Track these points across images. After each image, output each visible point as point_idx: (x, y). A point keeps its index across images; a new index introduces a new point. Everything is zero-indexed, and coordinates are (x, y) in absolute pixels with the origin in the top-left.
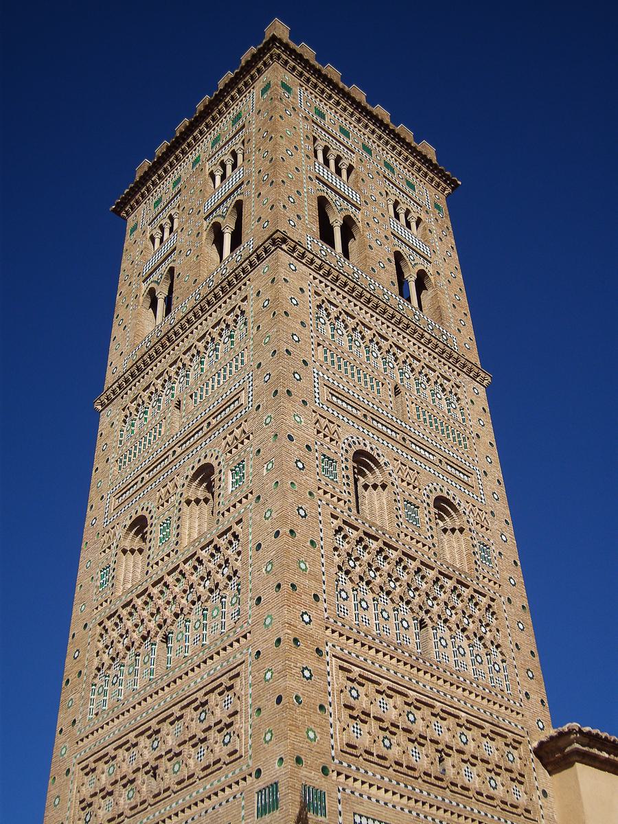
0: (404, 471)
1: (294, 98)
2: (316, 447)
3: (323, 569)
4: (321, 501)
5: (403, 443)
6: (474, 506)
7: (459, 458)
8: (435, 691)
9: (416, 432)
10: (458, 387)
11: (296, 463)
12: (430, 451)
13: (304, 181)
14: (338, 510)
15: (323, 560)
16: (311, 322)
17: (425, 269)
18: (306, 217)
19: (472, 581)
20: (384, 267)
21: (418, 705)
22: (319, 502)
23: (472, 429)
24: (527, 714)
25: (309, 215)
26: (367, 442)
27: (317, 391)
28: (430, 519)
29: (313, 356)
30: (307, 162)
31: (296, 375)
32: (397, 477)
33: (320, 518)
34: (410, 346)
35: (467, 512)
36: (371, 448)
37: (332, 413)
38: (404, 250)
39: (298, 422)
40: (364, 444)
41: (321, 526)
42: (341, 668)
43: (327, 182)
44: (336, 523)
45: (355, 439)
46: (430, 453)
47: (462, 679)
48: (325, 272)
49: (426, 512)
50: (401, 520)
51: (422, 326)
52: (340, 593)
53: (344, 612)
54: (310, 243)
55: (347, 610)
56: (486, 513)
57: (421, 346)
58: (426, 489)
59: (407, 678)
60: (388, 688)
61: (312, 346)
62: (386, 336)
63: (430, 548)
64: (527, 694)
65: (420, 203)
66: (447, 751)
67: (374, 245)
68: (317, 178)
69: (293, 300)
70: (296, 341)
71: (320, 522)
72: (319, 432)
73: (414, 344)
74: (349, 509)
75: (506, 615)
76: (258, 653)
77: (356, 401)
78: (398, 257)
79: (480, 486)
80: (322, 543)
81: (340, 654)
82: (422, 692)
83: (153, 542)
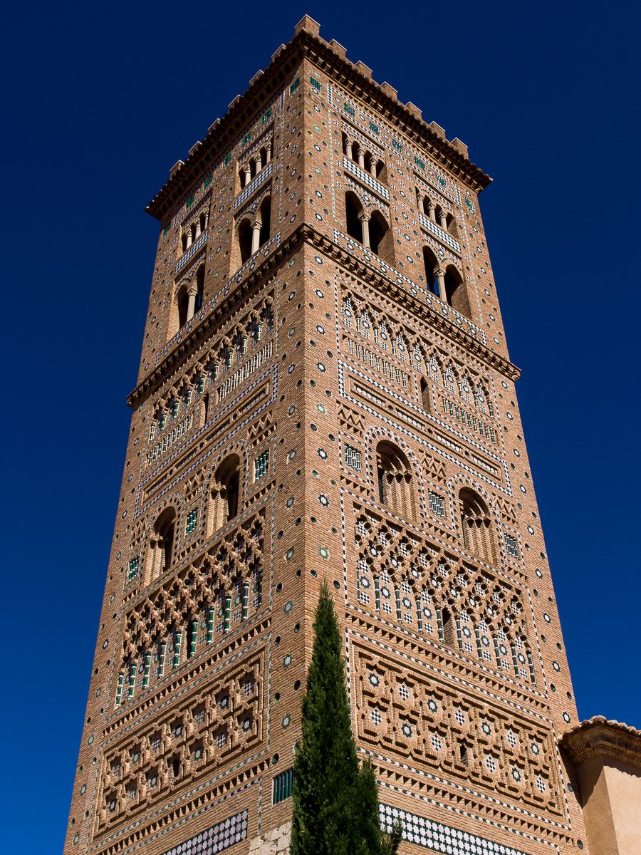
0: (428, 462)
1: (323, 94)
2: (340, 437)
3: (344, 556)
4: (343, 489)
5: (428, 434)
6: (501, 498)
7: (485, 450)
8: (457, 679)
9: (442, 424)
10: (487, 381)
11: (319, 451)
12: (456, 443)
13: (332, 176)
14: (361, 499)
15: (344, 548)
16: (336, 314)
17: (454, 264)
18: (334, 212)
19: (497, 572)
20: (412, 262)
21: (440, 693)
22: (342, 491)
23: (499, 422)
24: (552, 706)
25: (336, 209)
26: (392, 433)
27: (341, 382)
28: (455, 510)
29: (338, 347)
30: (335, 158)
31: (320, 366)
32: (421, 468)
33: (342, 506)
34: (437, 340)
35: (493, 504)
36: (396, 439)
37: (355, 404)
38: (433, 246)
39: (322, 412)
40: (389, 435)
41: (343, 514)
42: (361, 655)
43: (355, 177)
44: (358, 513)
45: (379, 429)
46: (456, 445)
47: (485, 669)
48: (351, 265)
49: (451, 503)
50: (425, 510)
51: (450, 320)
52: (361, 580)
53: (365, 600)
54: (336, 237)
55: (368, 598)
56: (513, 506)
57: (449, 340)
58: (451, 480)
59: (428, 666)
60: (409, 675)
61: (337, 338)
62: (413, 329)
63: (454, 539)
64: (552, 686)
65: (451, 199)
66: (469, 740)
67: (402, 240)
68: (346, 174)
69: (319, 293)
70: (321, 333)
71: (342, 510)
72: (342, 423)
73: (442, 338)
74: (372, 498)
75: (531, 607)
76: (278, 639)
77: (381, 392)
78: (428, 254)
79: (507, 478)
80: (343, 531)
81: (359, 640)
82: (442, 680)
83: (180, 533)
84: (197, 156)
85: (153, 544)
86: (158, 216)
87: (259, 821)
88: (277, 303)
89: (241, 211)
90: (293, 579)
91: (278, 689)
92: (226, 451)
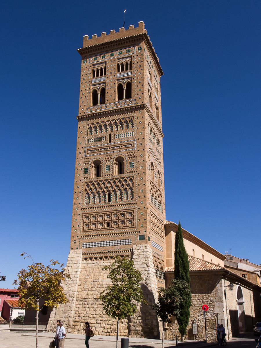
84: (100, 46)
85: (93, 167)
86: (81, 54)
87: (135, 242)
88: (135, 121)
89: (119, 80)
90: (143, 197)
91: (145, 221)
92: (119, 155)
